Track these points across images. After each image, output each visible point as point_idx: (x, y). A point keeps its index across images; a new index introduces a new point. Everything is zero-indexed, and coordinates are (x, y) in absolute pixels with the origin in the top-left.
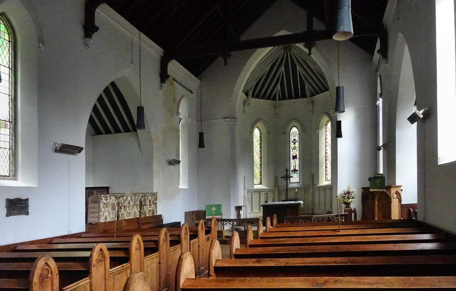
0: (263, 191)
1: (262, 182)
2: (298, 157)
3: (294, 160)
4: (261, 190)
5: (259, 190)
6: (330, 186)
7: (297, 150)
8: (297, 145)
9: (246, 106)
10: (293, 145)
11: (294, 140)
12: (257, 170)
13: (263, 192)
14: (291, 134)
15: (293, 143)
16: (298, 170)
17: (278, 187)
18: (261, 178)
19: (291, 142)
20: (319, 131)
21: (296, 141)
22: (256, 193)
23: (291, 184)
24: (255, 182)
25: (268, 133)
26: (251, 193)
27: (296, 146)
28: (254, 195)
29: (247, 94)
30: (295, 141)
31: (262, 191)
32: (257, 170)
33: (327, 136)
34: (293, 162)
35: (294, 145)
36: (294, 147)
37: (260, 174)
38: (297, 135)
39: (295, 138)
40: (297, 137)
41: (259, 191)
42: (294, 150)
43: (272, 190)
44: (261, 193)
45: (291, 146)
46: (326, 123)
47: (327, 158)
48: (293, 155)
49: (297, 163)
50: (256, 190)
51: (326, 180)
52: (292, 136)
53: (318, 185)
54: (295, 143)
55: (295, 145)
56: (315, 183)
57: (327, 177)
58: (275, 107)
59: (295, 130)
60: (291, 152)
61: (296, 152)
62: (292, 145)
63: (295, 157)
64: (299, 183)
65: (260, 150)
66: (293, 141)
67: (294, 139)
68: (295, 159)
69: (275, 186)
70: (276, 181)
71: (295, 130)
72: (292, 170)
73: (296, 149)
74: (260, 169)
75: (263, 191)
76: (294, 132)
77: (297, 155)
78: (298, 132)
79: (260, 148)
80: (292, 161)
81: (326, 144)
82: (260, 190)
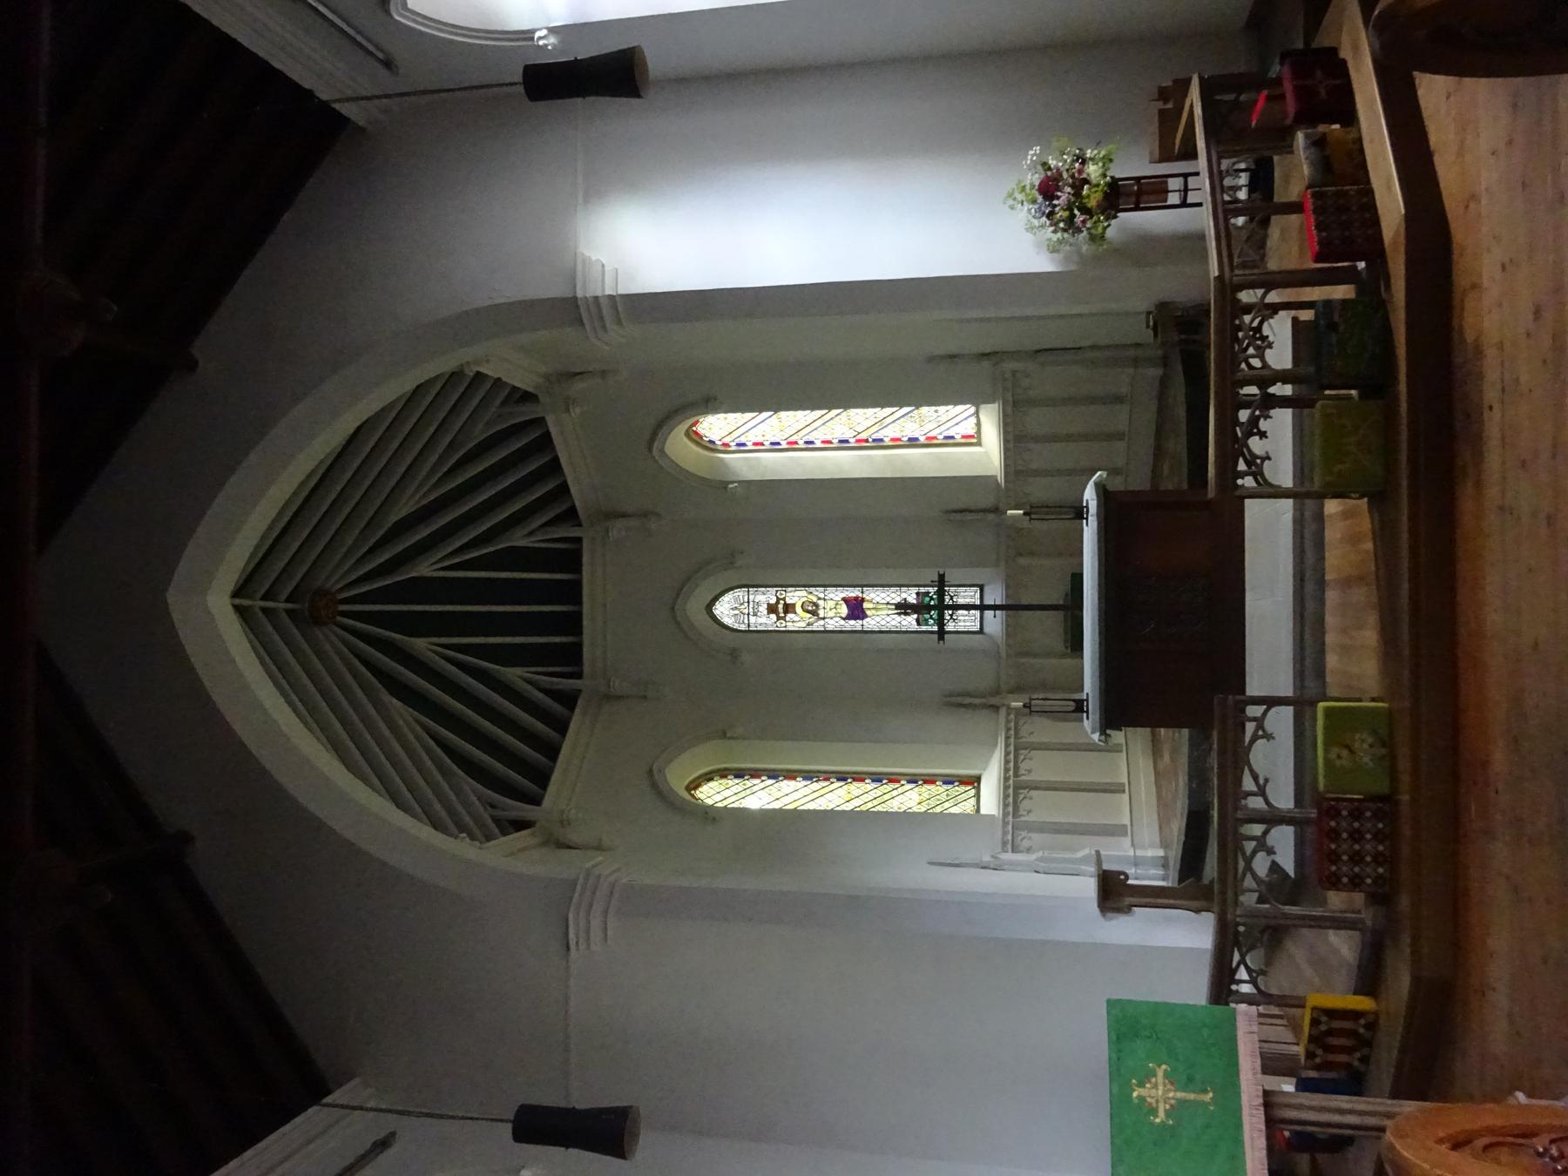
0: (1016, 768)
1: (966, 776)
2: (854, 593)
3: (868, 613)
4: (1006, 779)
5: (1006, 788)
6: (1009, 409)
7: (822, 595)
8: (796, 597)
9: (573, 836)
10: (796, 619)
11: (772, 609)
12: (909, 799)
13: (1022, 771)
14: (743, 627)
15: (790, 616)
16: (918, 594)
17: (997, 692)
18: (949, 780)
19: (781, 625)
20: (733, 482)
21: (778, 599)
22: (1025, 805)
23: (987, 629)
24: (968, 807)
25: (724, 735)
26: (1024, 834)
27: (805, 599)
28: (1032, 818)
29: (520, 825)
30: (781, 606)
31: (1016, 775)
32: (909, 799)
33: (762, 444)
34: (878, 619)
35: (796, 613)
36: (808, 612)
37: (926, 782)
38: (751, 597)
39: (766, 606)
40: (761, 598)
41: (1015, 789)
42: (821, 613)
43: (1012, 724)
44: (1023, 778)
45: (801, 625)
46: (698, 444)
47: (867, 441)
48: (844, 619)
49: (883, 595)
50: (1006, 805)
51: (974, 441)
52: (753, 620)
53: (1001, 479)
54: (789, 608)
55: (798, 609)
56: (988, 501)
57: (963, 437)
58: (609, 698)
59: (725, 609)
60: (830, 628)
61: (831, 604)
62: (798, 621)
63: (856, 609)
64: (986, 589)
65: (805, 779)
66: (779, 618)
67: (768, 613)
68: (866, 605)
69: (996, 708)
70: (968, 700)
71: (725, 609)
72: (914, 623)
73: (815, 600)
74: (897, 785)
75: (1016, 768)
76: (736, 607)
77: (843, 595)
78: (740, 593)
79: (794, 778)
80: (870, 623)
81: (801, 444)
82: (1011, 782)
